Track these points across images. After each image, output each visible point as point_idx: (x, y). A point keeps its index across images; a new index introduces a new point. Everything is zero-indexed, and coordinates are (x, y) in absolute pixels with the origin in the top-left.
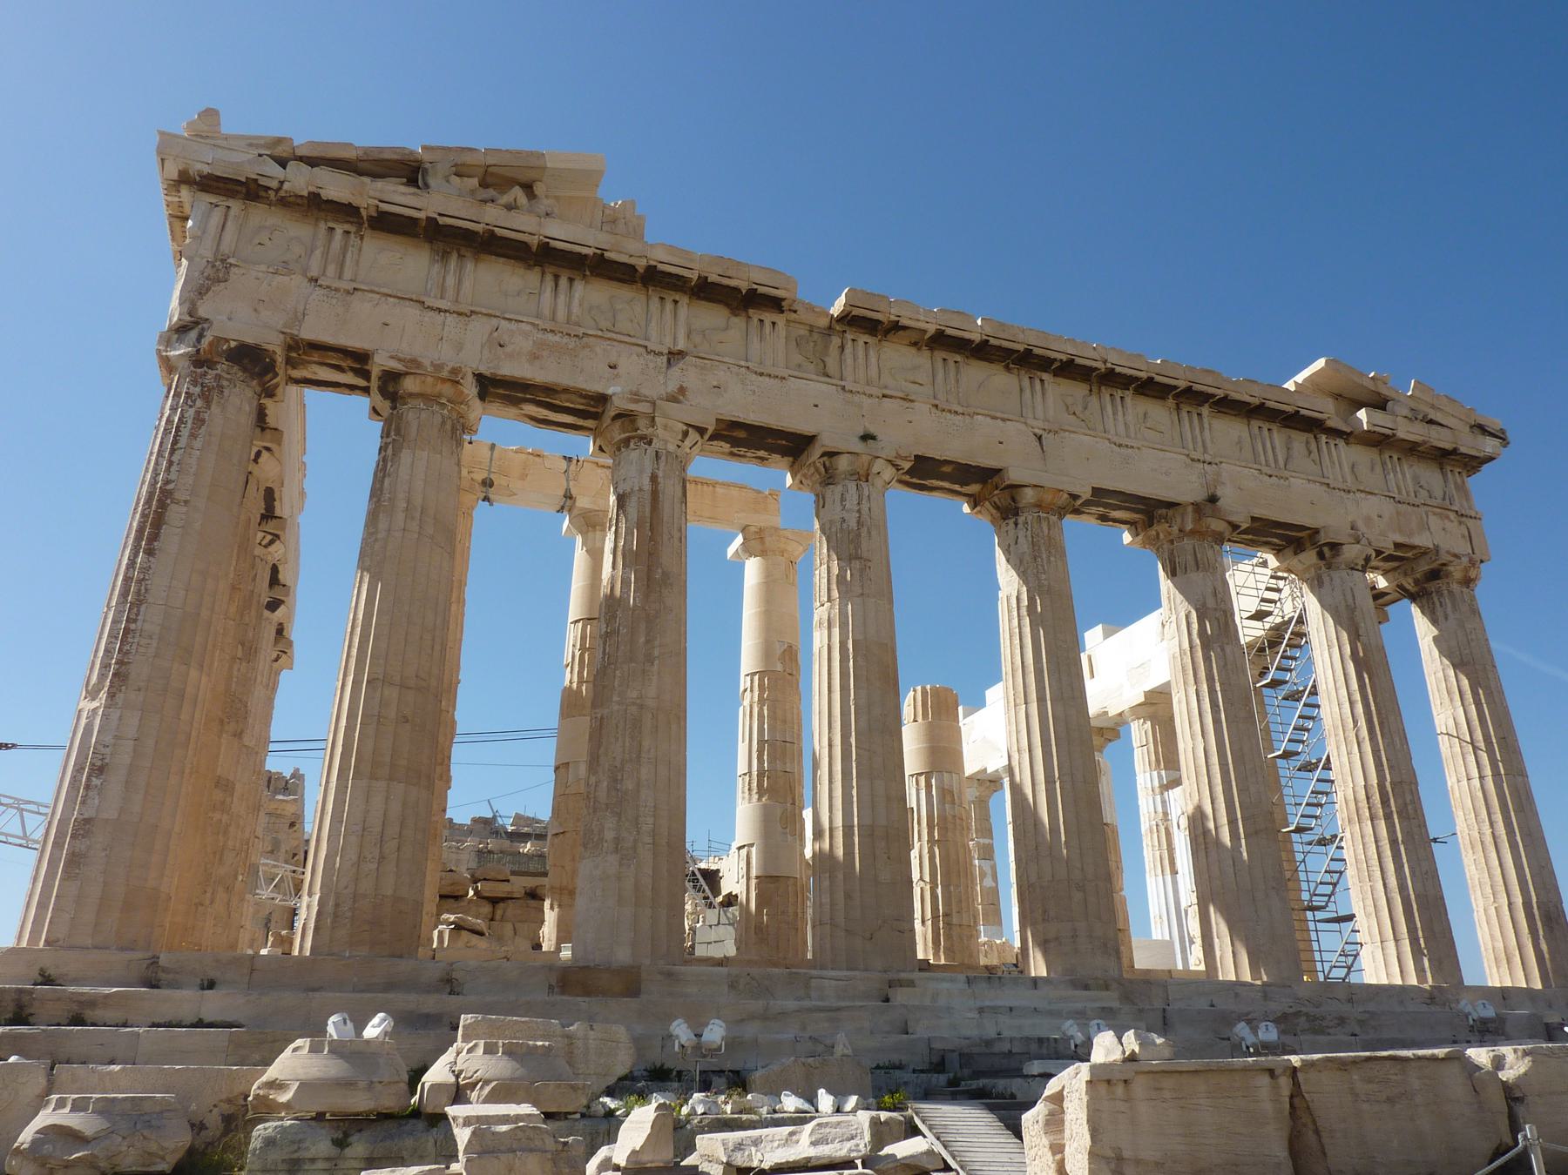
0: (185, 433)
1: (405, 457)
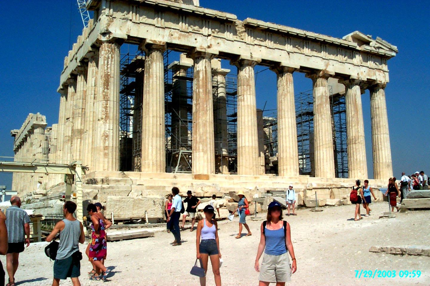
0: (110, 60)
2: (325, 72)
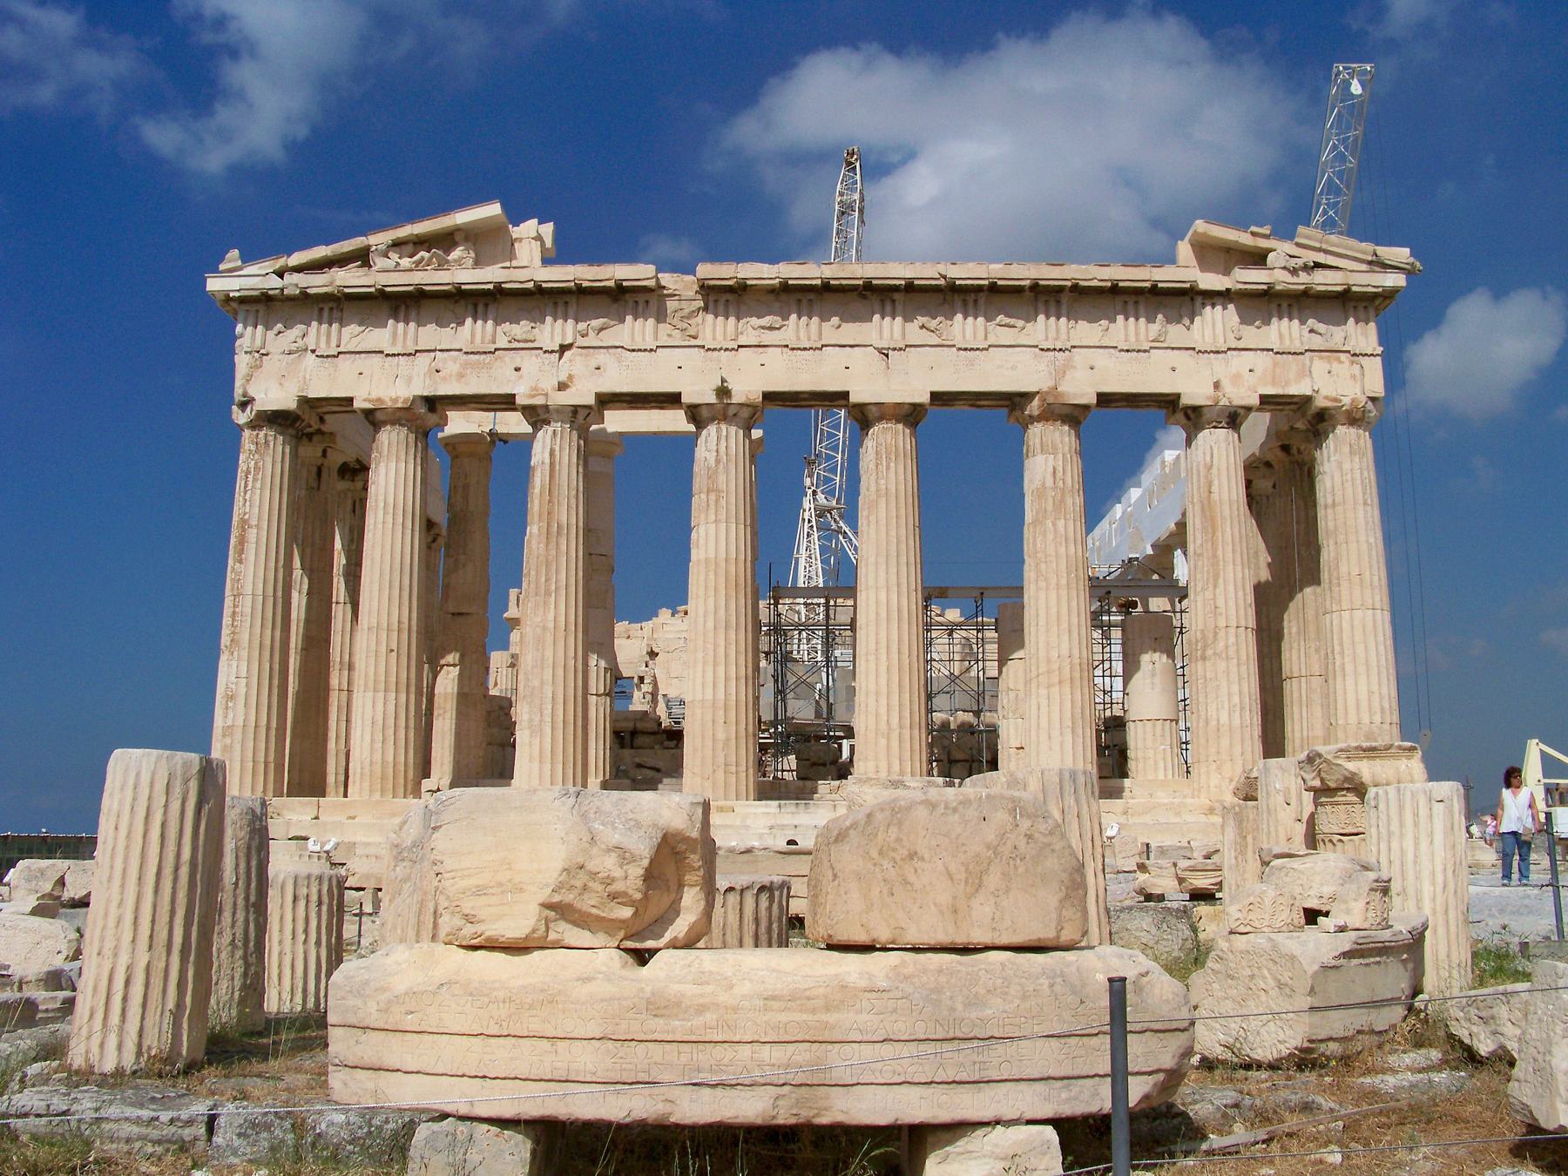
0: (251, 477)
1: (382, 469)
2: (1050, 400)
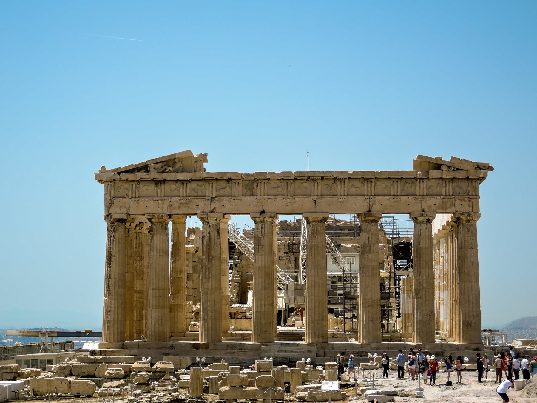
0: (112, 240)
1: (155, 237)
